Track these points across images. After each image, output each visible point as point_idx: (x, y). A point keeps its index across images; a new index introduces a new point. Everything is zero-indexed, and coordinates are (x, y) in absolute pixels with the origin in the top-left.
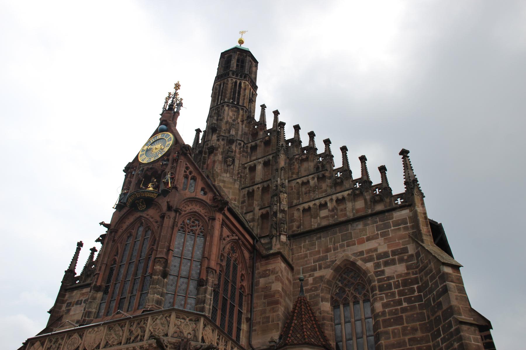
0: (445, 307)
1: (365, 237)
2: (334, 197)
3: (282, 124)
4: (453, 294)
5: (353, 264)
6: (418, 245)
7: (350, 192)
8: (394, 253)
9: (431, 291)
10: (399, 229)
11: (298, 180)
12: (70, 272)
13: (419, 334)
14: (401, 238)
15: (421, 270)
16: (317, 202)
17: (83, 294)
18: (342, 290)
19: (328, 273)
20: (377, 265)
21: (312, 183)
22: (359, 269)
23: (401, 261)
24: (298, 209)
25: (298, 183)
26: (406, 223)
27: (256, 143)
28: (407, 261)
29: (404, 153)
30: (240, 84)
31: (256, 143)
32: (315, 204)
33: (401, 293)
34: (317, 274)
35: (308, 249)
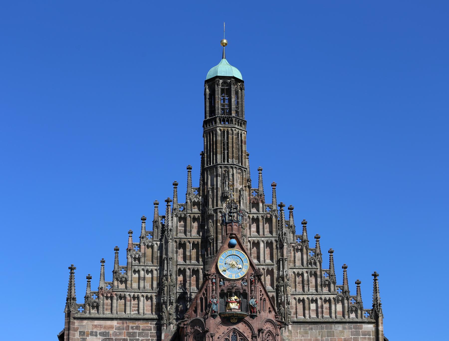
1: (343, 338)
2: (323, 297)
7: (335, 296)
10: (365, 338)
11: (294, 270)
12: (70, 299)
16: (310, 297)
17: (96, 326)
21: (305, 275)
24: (295, 299)
25: (294, 272)
26: (370, 335)
27: (257, 216)
30: (241, 135)
31: (257, 216)
32: (308, 298)
35: (303, 336)
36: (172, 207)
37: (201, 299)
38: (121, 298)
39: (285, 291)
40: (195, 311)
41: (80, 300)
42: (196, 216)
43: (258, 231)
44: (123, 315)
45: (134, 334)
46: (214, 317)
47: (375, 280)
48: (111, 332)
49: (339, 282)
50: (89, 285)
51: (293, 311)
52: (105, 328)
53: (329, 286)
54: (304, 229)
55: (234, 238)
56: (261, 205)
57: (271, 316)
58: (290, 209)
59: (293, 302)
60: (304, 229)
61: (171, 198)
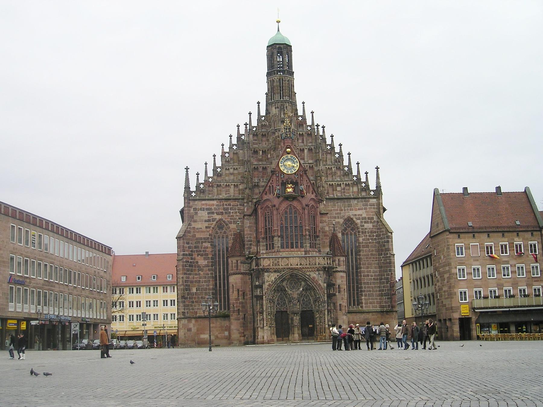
0: (386, 247)
2: (345, 183)
3: (318, 126)
4: (390, 243)
5: (352, 219)
6: (378, 218)
7: (352, 182)
8: (369, 218)
9: (381, 239)
12: (187, 188)
13: (374, 253)
14: (372, 212)
15: (378, 229)
18: (345, 229)
19: (341, 221)
20: (361, 222)
21: (333, 169)
22: (354, 221)
23: (371, 222)
28: (373, 223)
29: (377, 168)
33: (370, 236)
34: (337, 220)
36: (248, 128)
37: (270, 186)
38: (218, 186)
39: (321, 180)
40: (266, 194)
41: (193, 188)
42: (264, 134)
43: (303, 142)
44: (221, 197)
45: (227, 209)
46: (279, 197)
47: (377, 171)
48: (213, 208)
49: (355, 173)
50: (198, 179)
51: (326, 192)
52: (209, 205)
53: (348, 174)
54: (332, 141)
55: (289, 148)
56: (305, 126)
57: (313, 196)
58: (323, 127)
59: (326, 186)
60: (332, 141)
61: (248, 123)
